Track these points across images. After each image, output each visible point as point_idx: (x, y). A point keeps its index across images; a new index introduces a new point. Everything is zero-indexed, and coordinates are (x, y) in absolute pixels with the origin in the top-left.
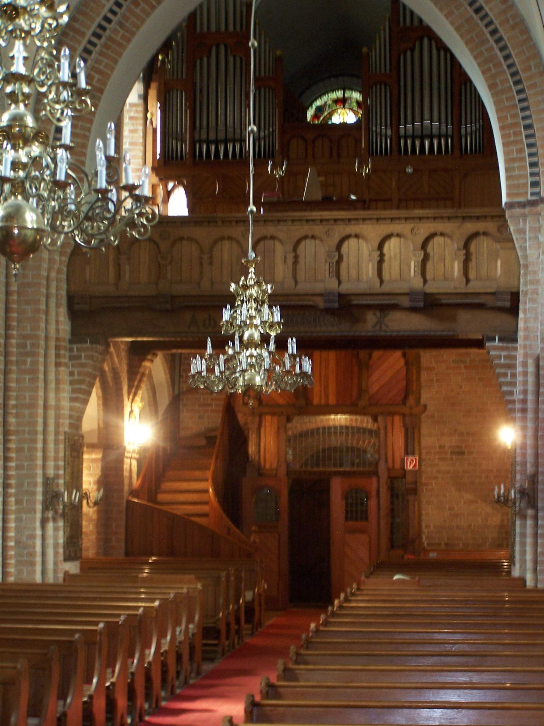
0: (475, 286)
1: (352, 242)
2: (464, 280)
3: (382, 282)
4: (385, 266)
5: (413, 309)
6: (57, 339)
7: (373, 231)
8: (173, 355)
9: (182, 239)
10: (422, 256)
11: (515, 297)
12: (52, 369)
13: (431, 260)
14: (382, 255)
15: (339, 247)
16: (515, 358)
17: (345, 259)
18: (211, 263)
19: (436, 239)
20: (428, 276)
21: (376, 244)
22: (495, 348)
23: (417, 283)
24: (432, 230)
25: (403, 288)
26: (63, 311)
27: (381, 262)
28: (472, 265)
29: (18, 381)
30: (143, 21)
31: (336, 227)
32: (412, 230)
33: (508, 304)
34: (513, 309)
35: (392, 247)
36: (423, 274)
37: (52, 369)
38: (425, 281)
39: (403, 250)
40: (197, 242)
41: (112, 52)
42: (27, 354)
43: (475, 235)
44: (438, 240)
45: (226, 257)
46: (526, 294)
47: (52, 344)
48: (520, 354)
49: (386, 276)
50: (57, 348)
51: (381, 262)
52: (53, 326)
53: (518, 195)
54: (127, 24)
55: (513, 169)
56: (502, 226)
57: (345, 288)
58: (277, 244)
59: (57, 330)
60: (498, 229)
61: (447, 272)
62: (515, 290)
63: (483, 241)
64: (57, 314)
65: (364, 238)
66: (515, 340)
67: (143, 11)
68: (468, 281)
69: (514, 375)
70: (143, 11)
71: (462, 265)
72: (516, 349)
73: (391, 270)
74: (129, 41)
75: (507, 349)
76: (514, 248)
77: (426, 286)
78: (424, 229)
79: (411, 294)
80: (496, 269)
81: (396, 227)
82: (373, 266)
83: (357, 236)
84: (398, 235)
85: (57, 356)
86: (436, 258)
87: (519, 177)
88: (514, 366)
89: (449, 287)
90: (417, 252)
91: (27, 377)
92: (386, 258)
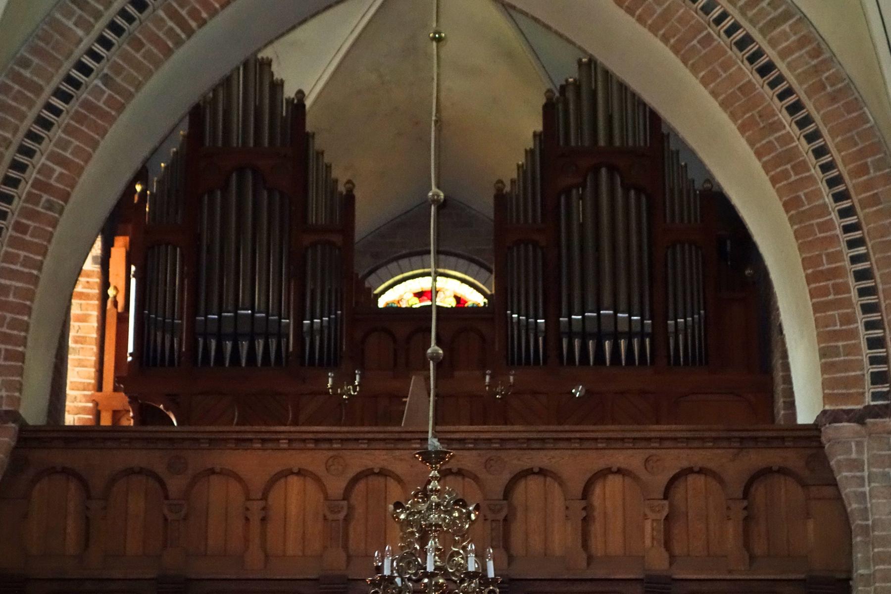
1: (533, 484)
3: (590, 559)
4: (596, 528)
9: (212, 472)
14: (588, 508)
15: (508, 492)
17: (520, 515)
19: (691, 478)
20: (677, 550)
21: (577, 488)
23: (658, 561)
24: (685, 464)
30: (149, 74)
31: (502, 454)
32: (647, 460)
35: (610, 495)
36: (667, 544)
43: (765, 472)
44: (696, 482)
49: (597, 546)
51: (587, 521)
53: (846, 398)
54: (118, 80)
55: (835, 352)
57: (519, 571)
58: (392, 484)
67: (148, 56)
68: (752, 558)
70: (148, 56)
73: (609, 539)
74: (121, 108)
81: (620, 458)
87: (847, 366)
90: (656, 503)
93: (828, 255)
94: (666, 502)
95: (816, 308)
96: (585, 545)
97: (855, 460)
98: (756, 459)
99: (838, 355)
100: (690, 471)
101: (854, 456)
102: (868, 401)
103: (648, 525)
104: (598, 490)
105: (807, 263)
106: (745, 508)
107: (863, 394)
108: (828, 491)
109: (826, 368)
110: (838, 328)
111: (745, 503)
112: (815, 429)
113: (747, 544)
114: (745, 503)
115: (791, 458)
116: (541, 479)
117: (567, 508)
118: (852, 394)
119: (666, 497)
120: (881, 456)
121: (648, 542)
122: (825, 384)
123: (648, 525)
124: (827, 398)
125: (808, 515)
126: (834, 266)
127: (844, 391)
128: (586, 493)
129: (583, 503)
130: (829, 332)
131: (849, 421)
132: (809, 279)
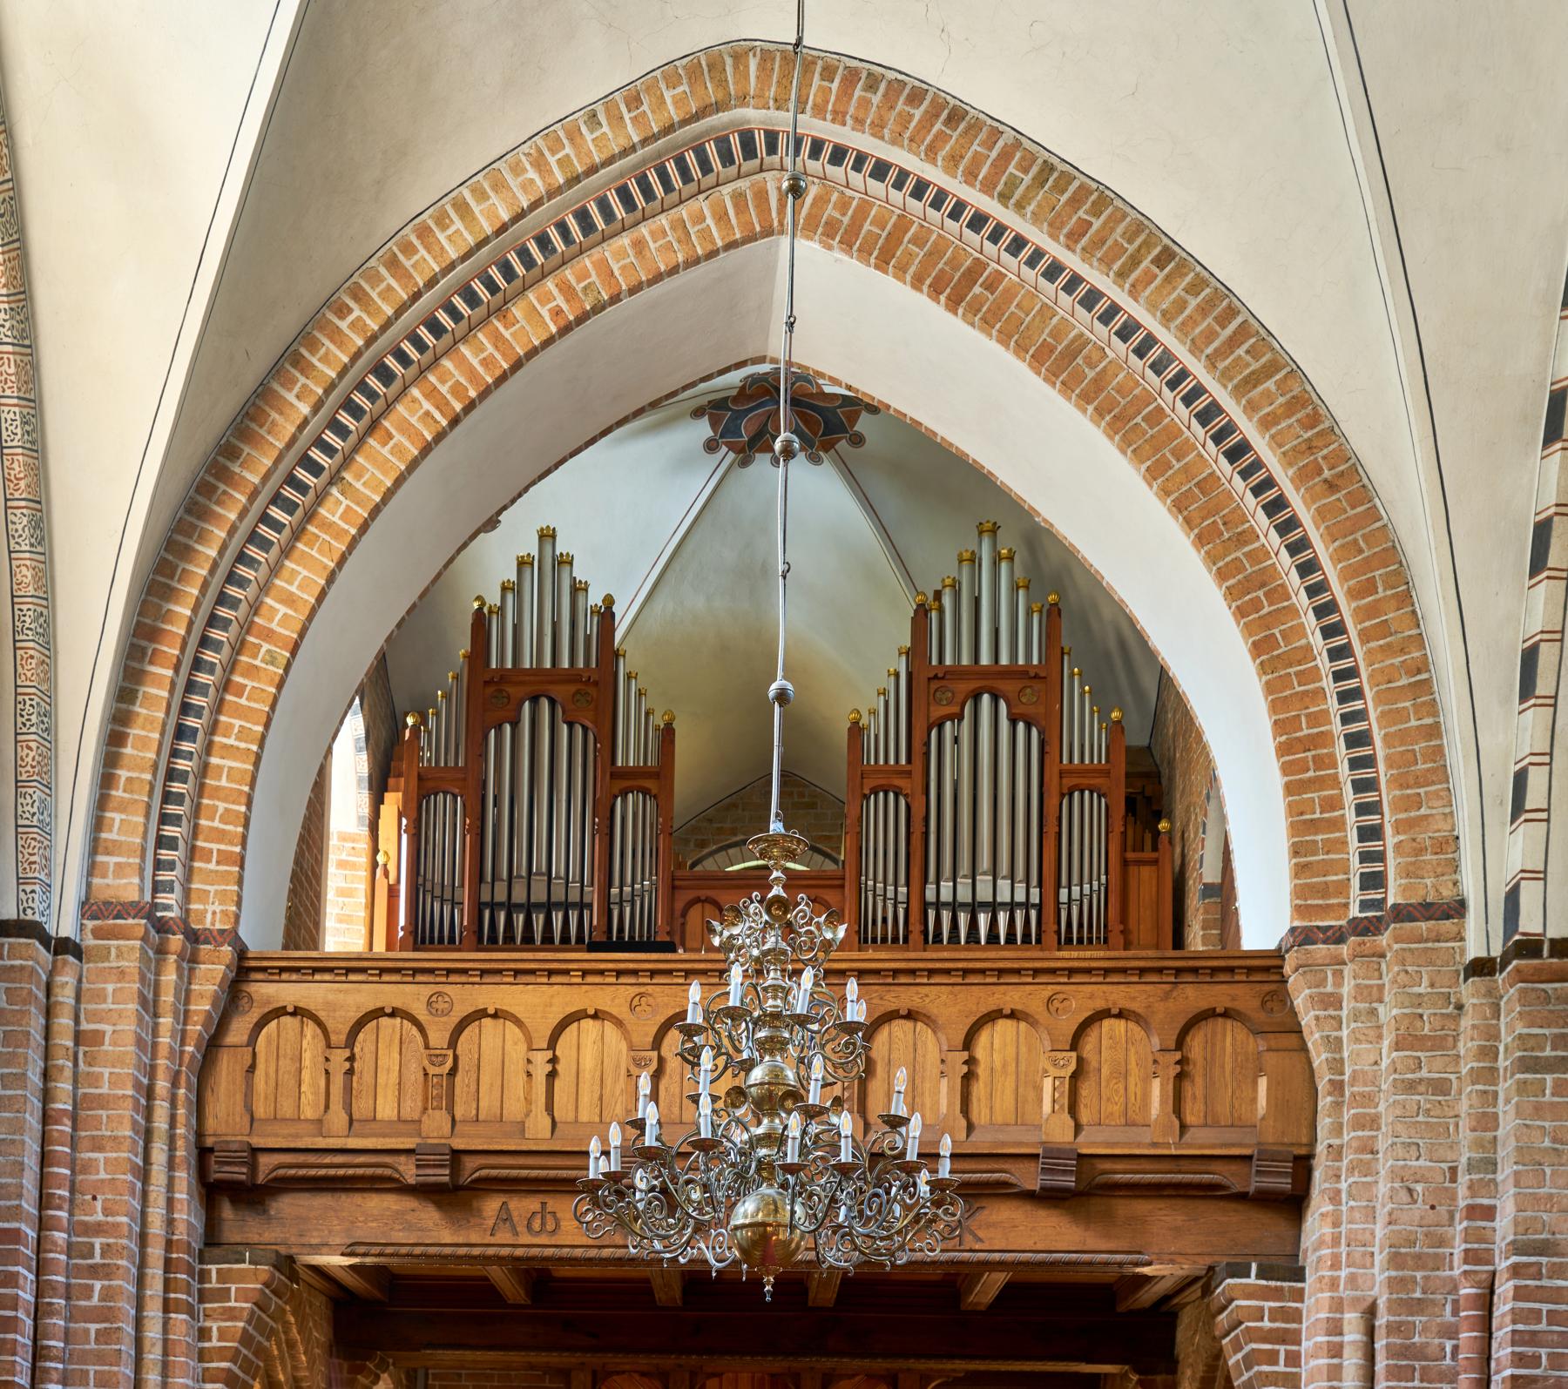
0: (1202, 1141)
2: (1177, 1123)
4: (979, 1090)
5: (1048, 1198)
6: (169, 1245)
7: (952, 1005)
8: (849, 420)
10: (1073, 1067)
11: (1303, 1165)
12: (154, 1312)
13: (1093, 1078)
14: (971, 1062)
16: (1296, 1316)
17: (880, 1069)
18: (552, 1075)
19: (1106, 1023)
20: (1085, 1116)
22: (1251, 1293)
23: (1059, 1131)
24: (1100, 1004)
25: (1026, 1141)
26: (182, 1175)
27: (968, 1078)
28: (1195, 1089)
29: (67, 1336)
32: (1050, 1000)
33: (1284, 1184)
34: (1293, 1204)
35: (998, 1042)
36: (1073, 1110)
37: (154, 1312)
38: (1078, 1128)
39: (1023, 1049)
40: (518, 1022)
41: (320, 551)
42: (94, 1271)
43: (1209, 1014)
44: (1112, 1028)
45: (588, 1062)
46: (1336, 1152)
47: (156, 1252)
48: (1315, 1305)
50: (168, 1265)
51: (968, 1078)
52: (157, 1213)
56: (1272, 993)
59: (170, 1223)
60: (1263, 1003)
61: (1136, 1106)
62: (1303, 1151)
63: (1225, 1029)
64: (170, 1187)
65: (929, 1020)
66: (1299, 1275)
68: (1183, 1128)
69: (1294, 1359)
71: (1170, 1087)
72: (1299, 1296)
73: (995, 1103)
75: (1277, 1294)
76: (1304, 1048)
77: (1081, 1139)
78: (1082, 999)
79: (1049, 1157)
80: (1254, 1100)
81: (1011, 997)
82: (951, 1089)
83: (910, 1016)
84: (1013, 1015)
85: (168, 1285)
86: (1105, 1071)
88: (1293, 1338)
89: (1141, 1142)
90: (1060, 1055)
91: (93, 1327)
92: (981, 1070)
93: (1308, 716)
94: (1074, 1054)
95: (1290, 789)
96: (965, 1110)
97: (1332, 994)
98: (1194, 996)
99: (1315, 853)
100: (1103, 1014)
101: (1329, 989)
102: (1354, 911)
103: (1048, 1084)
104: (983, 1038)
105: (1279, 727)
106: (1178, 1063)
107: (1346, 905)
108: (1292, 1040)
109: (1300, 870)
110: (1317, 815)
111: (1178, 1056)
112: (1278, 954)
113: (1178, 1110)
114: (1178, 1056)
115: (1243, 996)
116: (909, 1025)
117: (943, 1061)
118: (1332, 905)
119: (1074, 1046)
120: (1367, 986)
121: (1047, 1106)
122: (1299, 892)
123: (1048, 1084)
124: (1299, 910)
125: (1260, 1070)
126: (1315, 730)
127: (1320, 902)
128: (968, 1043)
129: (965, 1055)
130: (1305, 822)
131: (1324, 942)
132: (1282, 750)
